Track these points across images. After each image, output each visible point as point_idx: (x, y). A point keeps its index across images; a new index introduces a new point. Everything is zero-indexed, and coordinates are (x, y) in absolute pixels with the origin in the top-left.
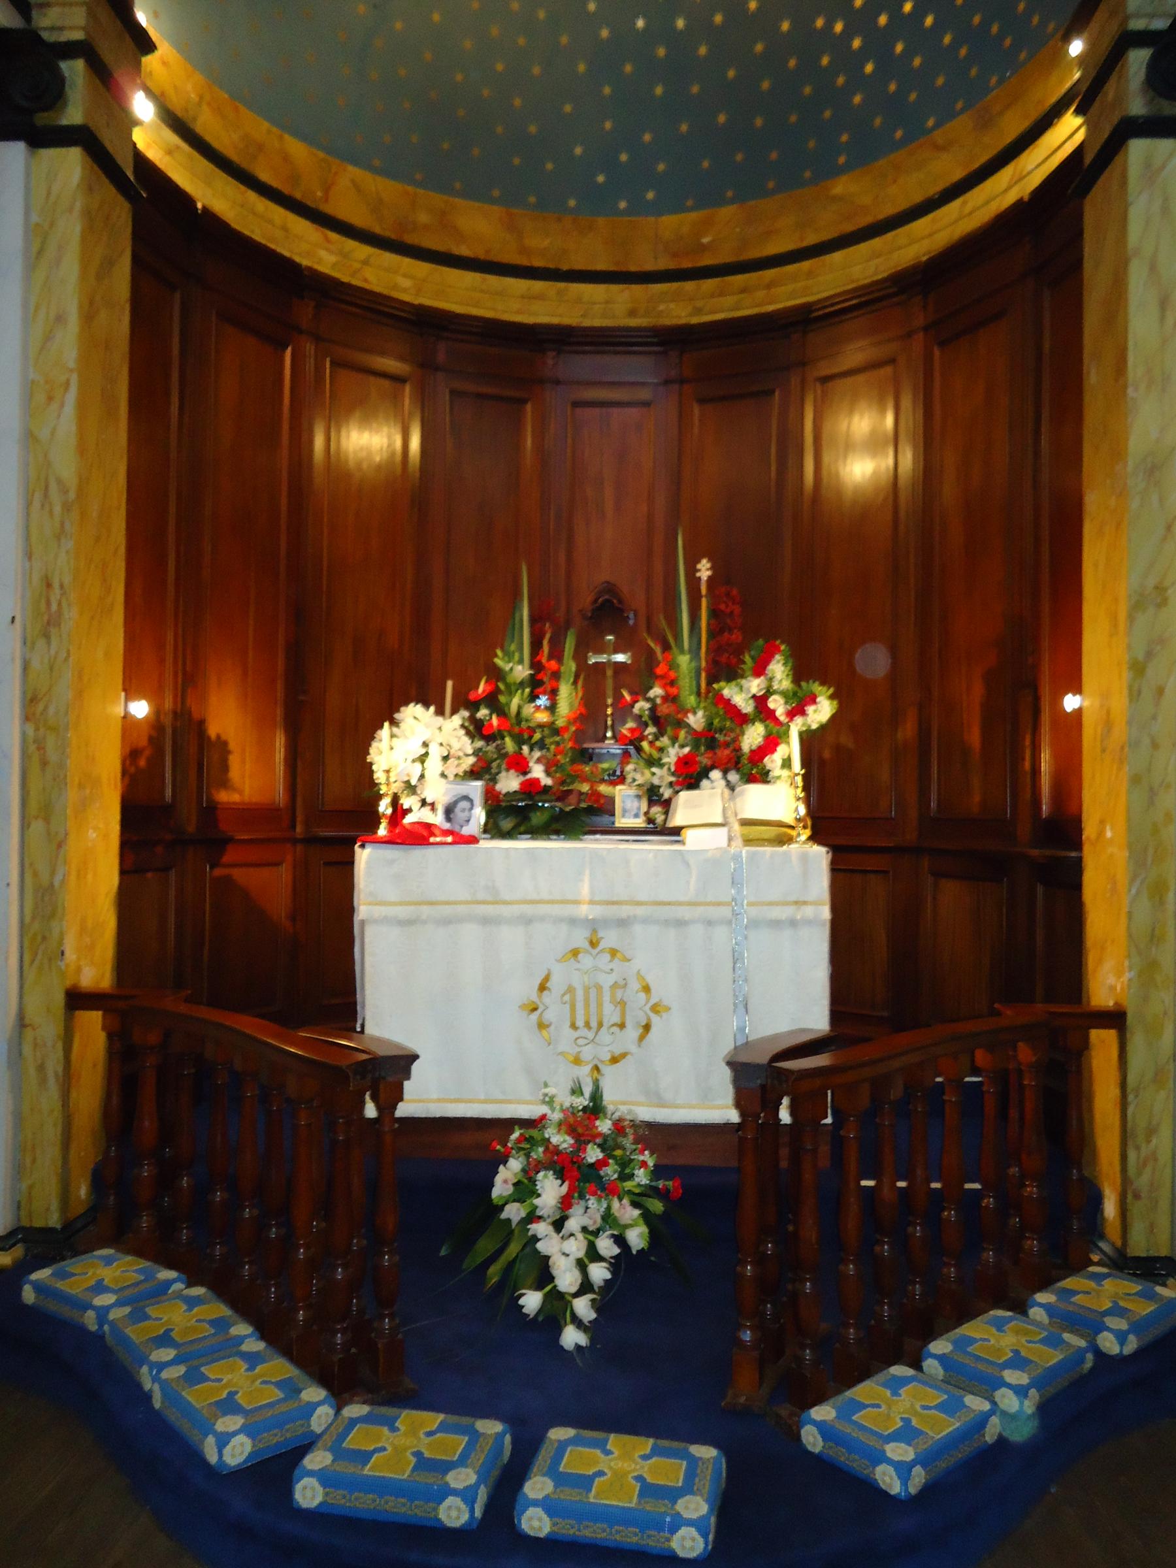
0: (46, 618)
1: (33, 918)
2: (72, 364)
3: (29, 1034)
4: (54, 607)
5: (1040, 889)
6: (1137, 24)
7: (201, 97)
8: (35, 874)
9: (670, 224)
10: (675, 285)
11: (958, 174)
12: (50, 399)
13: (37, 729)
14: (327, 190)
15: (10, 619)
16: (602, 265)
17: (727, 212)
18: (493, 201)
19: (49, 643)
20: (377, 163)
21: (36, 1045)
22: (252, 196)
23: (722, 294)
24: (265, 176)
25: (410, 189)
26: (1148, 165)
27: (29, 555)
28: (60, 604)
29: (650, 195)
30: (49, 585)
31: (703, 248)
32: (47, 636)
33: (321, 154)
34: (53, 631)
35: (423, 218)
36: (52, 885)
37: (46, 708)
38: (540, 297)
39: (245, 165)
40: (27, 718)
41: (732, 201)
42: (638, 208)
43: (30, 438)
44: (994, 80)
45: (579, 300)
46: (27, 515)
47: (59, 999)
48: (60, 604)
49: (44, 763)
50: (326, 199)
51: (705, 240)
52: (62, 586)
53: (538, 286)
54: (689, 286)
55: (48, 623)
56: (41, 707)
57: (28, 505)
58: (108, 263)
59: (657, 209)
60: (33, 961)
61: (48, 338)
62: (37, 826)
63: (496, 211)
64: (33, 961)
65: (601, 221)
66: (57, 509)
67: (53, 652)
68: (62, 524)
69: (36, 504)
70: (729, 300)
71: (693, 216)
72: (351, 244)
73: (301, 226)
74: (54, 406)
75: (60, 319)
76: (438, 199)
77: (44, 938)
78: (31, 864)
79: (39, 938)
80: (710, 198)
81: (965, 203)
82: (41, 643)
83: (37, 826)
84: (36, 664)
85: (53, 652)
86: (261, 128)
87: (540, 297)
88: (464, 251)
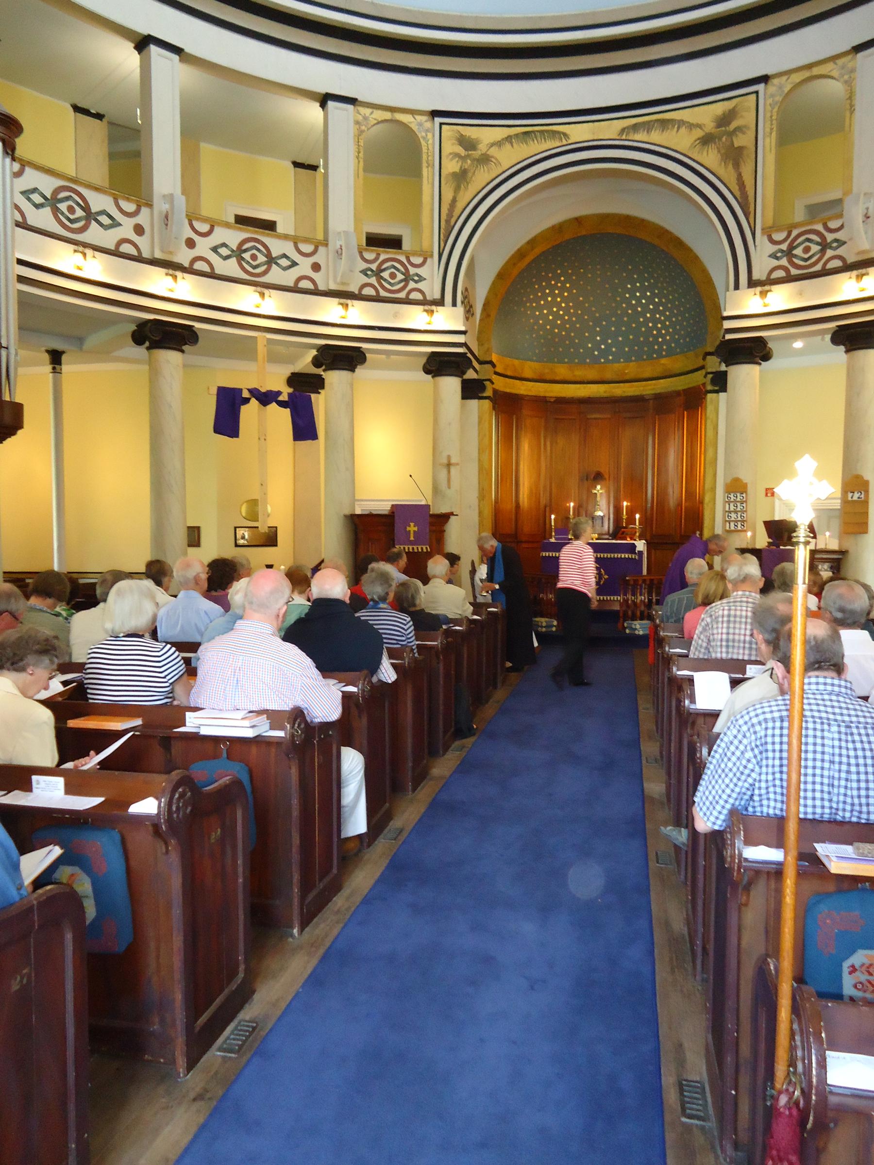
6: (709, 370)
11: (690, 368)
17: (632, 364)
18: (565, 363)
24: (509, 373)
31: (626, 374)
35: (547, 371)
40: (480, 516)
41: (634, 361)
42: (607, 361)
43: (479, 460)
54: (622, 385)
59: (613, 361)
65: (596, 366)
71: (623, 364)
80: (627, 360)
84: (481, 505)
87: (579, 389)
88: (557, 378)
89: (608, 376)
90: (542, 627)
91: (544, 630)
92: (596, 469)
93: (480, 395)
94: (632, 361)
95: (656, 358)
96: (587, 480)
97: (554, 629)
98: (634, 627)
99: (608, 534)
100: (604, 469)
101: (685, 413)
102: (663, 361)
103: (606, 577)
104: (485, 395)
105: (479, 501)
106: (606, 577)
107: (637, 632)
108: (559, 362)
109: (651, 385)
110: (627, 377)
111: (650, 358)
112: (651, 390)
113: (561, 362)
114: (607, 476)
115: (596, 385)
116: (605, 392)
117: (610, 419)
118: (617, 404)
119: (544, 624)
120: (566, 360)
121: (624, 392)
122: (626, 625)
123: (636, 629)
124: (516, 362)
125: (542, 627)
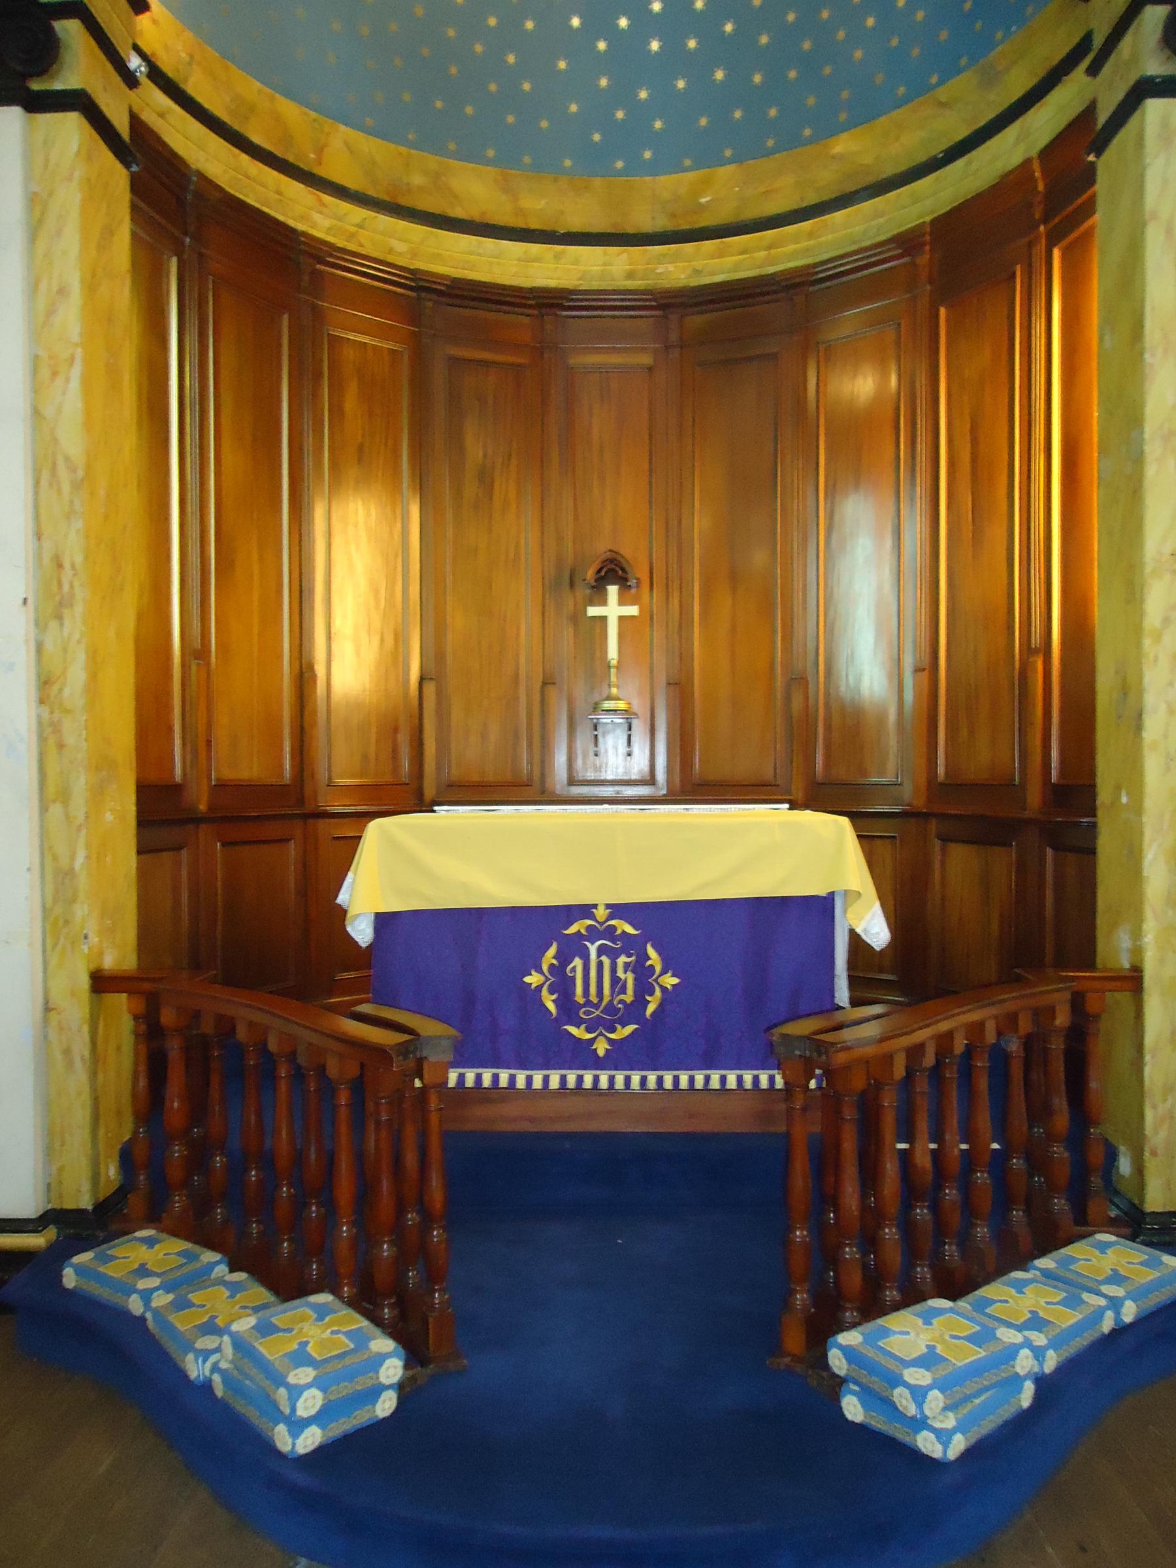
0: (57, 598)
1: (55, 901)
2: (76, 338)
3: (54, 1017)
4: (66, 588)
5: (1049, 852)
7: (192, 57)
8: (55, 858)
9: (669, 184)
10: (673, 247)
11: (962, 133)
12: (55, 374)
13: (52, 713)
14: (320, 151)
15: (21, 601)
16: (599, 225)
17: (725, 172)
18: (488, 162)
19: (62, 625)
20: (369, 121)
21: (61, 1028)
22: (245, 158)
23: (721, 256)
24: (256, 139)
25: (403, 150)
26: (1165, 124)
27: (38, 536)
28: (72, 586)
29: (647, 155)
30: (60, 566)
31: (702, 208)
32: (59, 618)
33: (313, 114)
34: (66, 612)
35: (417, 180)
36: (72, 870)
37: (60, 690)
38: (538, 259)
39: (236, 126)
41: (730, 161)
42: (636, 168)
43: (36, 413)
44: (999, 35)
45: (576, 262)
46: (36, 494)
47: (84, 982)
48: (72, 586)
49: (61, 746)
50: (319, 162)
51: (703, 200)
52: (73, 567)
53: (535, 248)
54: (688, 247)
55: (61, 604)
56: (55, 688)
57: (37, 483)
58: (109, 232)
59: (654, 169)
60: (55, 945)
61: (51, 312)
62: (56, 810)
63: (491, 171)
64: (55, 945)
65: (597, 182)
66: (66, 488)
67: (66, 634)
68: (72, 502)
69: (44, 483)
70: (730, 261)
71: (691, 176)
72: (345, 207)
73: (295, 189)
74: (59, 381)
75: (62, 291)
76: (433, 161)
77: (67, 922)
78: (51, 848)
79: (61, 922)
80: (708, 159)
81: (969, 163)
82: (53, 625)
83: (56, 810)
84: (49, 646)
85: (66, 634)
86: (251, 88)
87: (538, 259)
88: (458, 212)
89: (644, 220)
90: (297, 1426)
91: (310, 1440)
92: (602, 547)
93: (36, 86)
94: (723, 162)
95: (811, 141)
96: (572, 585)
97: (386, 1405)
98: (902, 1398)
99: (651, 780)
100: (634, 552)
101: (943, 311)
102: (842, 145)
103: (670, 981)
104: (60, 84)
105: (40, 624)
106: (670, 981)
107: (927, 1444)
108: (459, 156)
109: (796, 239)
110: (706, 220)
111: (791, 141)
112: (793, 255)
113: (470, 155)
114: (640, 571)
115: (599, 250)
116: (630, 275)
117: (650, 369)
118: (674, 317)
119: (310, 1403)
120: (491, 153)
121: (697, 272)
122: (837, 1361)
123: (920, 1423)
124: (290, 110)
125: (297, 1426)
